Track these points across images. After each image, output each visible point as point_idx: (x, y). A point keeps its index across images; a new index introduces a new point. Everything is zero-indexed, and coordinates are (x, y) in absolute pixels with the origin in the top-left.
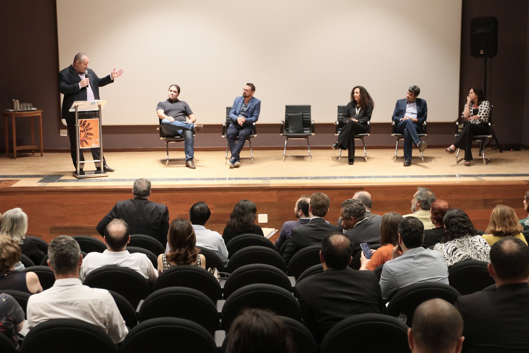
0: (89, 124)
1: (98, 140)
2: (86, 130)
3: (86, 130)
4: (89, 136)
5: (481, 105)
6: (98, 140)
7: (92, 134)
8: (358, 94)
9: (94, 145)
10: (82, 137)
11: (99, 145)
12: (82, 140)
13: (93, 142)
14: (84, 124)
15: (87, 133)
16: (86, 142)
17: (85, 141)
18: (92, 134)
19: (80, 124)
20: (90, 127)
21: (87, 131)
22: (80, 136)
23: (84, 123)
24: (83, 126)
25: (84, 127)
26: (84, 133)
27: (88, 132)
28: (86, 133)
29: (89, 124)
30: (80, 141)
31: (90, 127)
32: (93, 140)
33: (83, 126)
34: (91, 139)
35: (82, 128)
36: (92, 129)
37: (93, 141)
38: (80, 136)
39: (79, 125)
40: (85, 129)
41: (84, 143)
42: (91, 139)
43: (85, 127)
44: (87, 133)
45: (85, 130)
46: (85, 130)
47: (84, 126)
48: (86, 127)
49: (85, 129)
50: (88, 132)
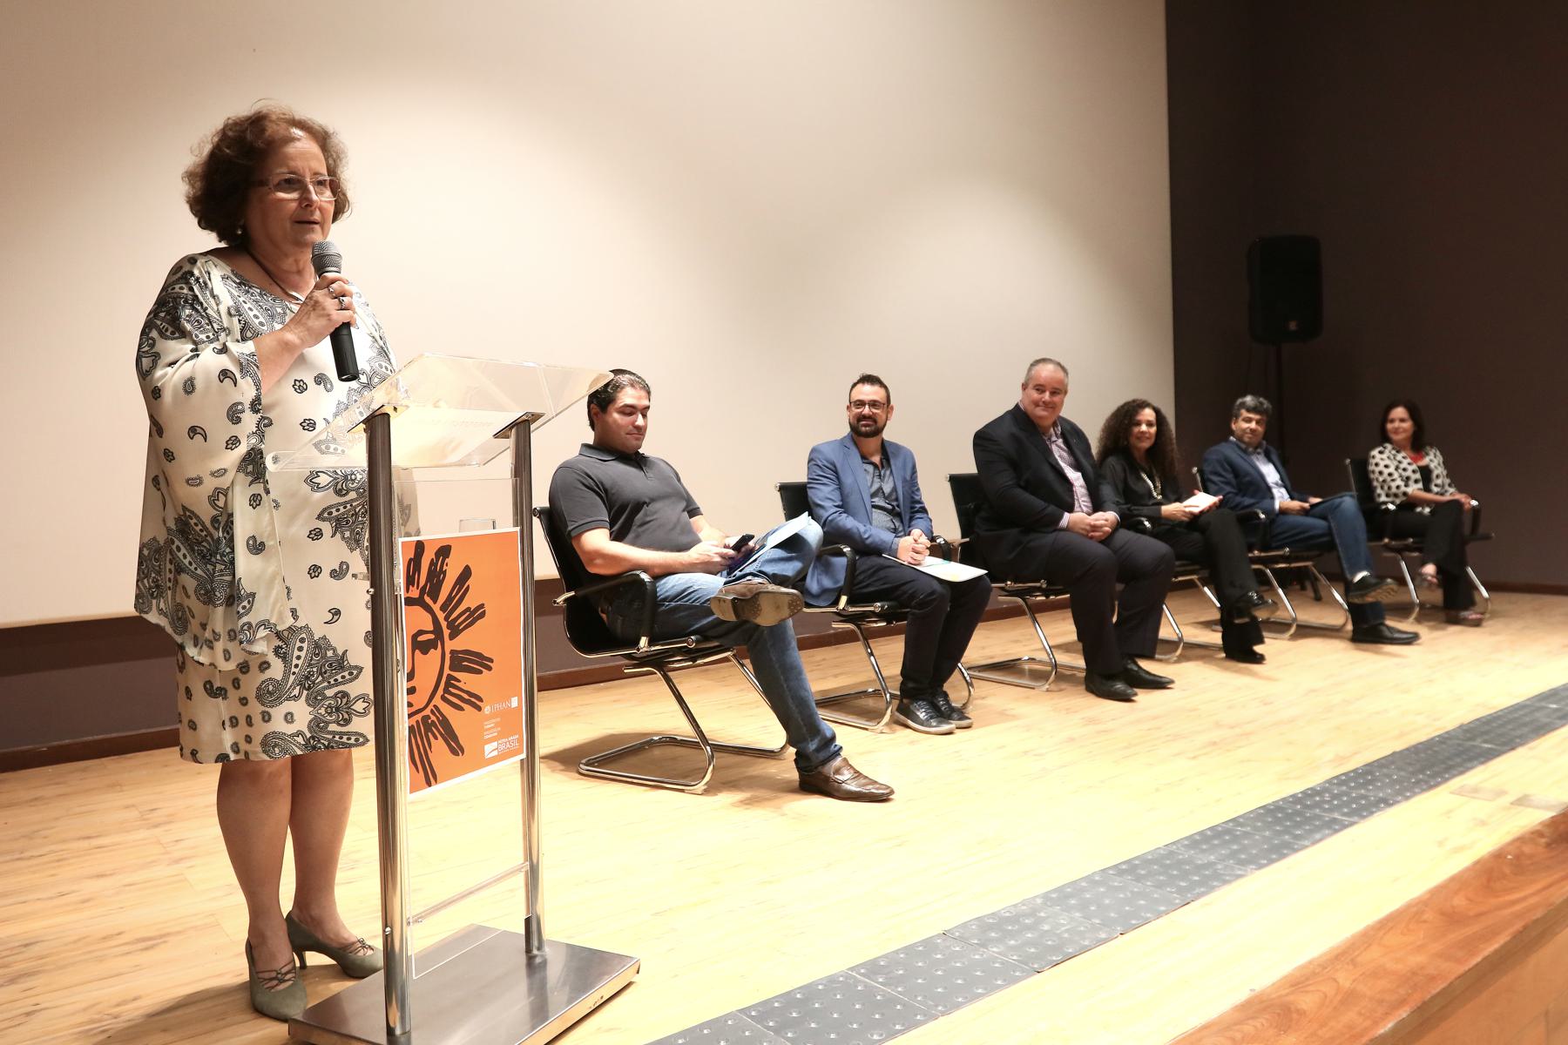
0: (466, 574)
1: (514, 702)
2: (446, 632)
3: (446, 632)
4: (466, 680)
5: (1374, 461)
6: (514, 702)
7: (476, 662)
8: (1153, 430)
9: (495, 744)
10: (420, 699)
11: (520, 740)
12: (426, 718)
13: (489, 725)
14: (436, 576)
15: (452, 652)
16: (450, 736)
17: (445, 722)
18: (476, 662)
19: (410, 581)
20: (470, 602)
21: (452, 637)
22: (412, 683)
23: (432, 563)
24: (427, 599)
25: (436, 608)
26: (435, 654)
27: (462, 642)
28: (448, 656)
29: (466, 574)
30: (411, 729)
31: (470, 602)
32: (487, 710)
33: (427, 599)
34: (474, 701)
35: (418, 609)
36: (483, 615)
37: (488, 718)
38: (412, 683)
39: (402, 593)
40: (441, 616)
41: (439, 747)
42: (474, 701)
43: (443, 608)
44: (452, 652)
45: (444, 624)
46: (444, 624)
47: (435, 602)
48: (450, 599)
49: (441, 616)
50: (462, 642)
